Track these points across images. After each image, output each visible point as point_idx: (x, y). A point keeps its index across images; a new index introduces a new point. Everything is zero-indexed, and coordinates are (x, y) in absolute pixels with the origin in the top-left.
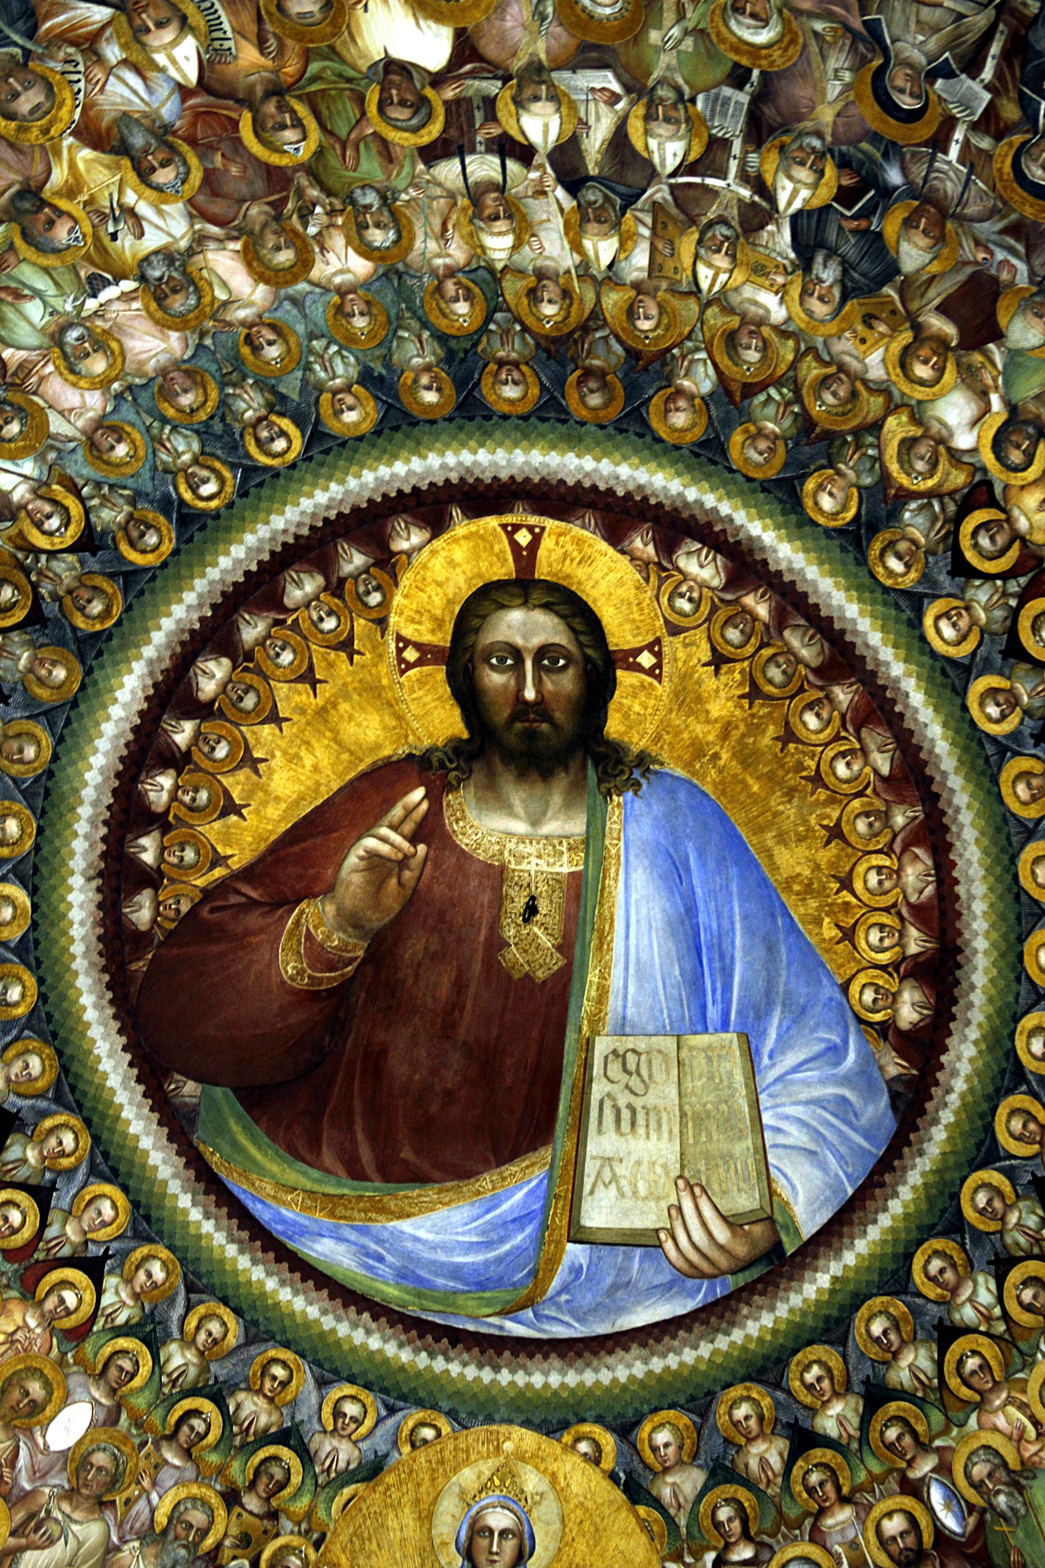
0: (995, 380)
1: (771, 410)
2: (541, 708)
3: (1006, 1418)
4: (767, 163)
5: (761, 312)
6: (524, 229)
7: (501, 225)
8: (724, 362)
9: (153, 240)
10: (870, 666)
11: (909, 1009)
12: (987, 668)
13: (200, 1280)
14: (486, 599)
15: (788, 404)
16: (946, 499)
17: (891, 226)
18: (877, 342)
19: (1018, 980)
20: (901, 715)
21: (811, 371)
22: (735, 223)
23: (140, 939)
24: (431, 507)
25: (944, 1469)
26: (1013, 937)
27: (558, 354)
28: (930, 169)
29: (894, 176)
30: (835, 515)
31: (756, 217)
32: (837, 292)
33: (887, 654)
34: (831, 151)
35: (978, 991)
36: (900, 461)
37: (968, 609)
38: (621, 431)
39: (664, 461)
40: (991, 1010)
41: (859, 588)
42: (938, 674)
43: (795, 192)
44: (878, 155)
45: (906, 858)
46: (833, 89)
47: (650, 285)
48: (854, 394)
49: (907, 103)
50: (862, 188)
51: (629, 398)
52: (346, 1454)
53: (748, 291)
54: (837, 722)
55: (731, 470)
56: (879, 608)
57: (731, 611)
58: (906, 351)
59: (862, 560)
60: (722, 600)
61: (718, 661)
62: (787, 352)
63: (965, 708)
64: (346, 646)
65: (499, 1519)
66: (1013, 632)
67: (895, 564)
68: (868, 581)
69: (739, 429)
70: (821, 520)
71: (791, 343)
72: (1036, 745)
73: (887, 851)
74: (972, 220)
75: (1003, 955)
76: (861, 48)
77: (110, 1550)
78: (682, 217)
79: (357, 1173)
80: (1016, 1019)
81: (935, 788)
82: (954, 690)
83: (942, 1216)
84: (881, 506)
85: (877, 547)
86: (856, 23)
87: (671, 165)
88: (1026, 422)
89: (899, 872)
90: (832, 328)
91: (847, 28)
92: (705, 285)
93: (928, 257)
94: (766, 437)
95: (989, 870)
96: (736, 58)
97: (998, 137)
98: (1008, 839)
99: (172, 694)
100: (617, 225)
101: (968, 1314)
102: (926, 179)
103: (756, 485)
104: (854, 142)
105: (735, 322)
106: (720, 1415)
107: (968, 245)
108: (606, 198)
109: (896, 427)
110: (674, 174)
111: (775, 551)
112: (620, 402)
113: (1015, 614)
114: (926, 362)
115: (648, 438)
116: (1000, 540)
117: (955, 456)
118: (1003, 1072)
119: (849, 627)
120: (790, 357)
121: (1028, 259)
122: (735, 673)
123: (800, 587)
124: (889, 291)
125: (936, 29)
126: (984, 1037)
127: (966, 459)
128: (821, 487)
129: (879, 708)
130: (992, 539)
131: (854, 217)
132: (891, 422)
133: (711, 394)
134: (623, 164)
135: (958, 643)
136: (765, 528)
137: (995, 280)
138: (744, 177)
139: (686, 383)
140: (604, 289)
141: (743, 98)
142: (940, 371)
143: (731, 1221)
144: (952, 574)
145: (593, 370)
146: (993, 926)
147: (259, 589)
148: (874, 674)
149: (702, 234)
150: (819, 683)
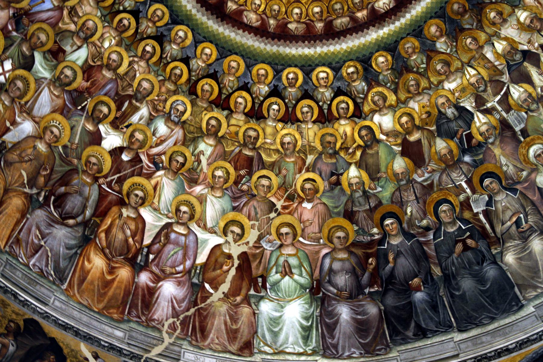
0: (390, 142)
1: (419, 61)
4: (493, 120)
5: (450, 80)
6: (522, 27)
7: (528, 21)
8: (442, 57)
10: (324, 41)
12: (305, 82)
15: (418, 68)
16: (362, 100)
17: (453, 145)
18: (421, 111)
19: (204, 37)
20: (304, 42)
21: (424, 83)
22: (482, 94)
26: (219, 43)
28: (463, 173)
29: (467, 159)
30: (376, 59)
31: (480, 102)
32: (443, 110)
33: (325, 49)
34: (486, 143)
35: (206, 20)
36: (381, 93)
37: (326, 86)
38: (441, 8)
39: (423, 15)
40: (199, 22)
41: (350, 53)
42: (311, 63)
43: (480, 121)
44: (476, 158)
45: (259, 17)
46: (503, 160)
47: (480, 51)
48: (409, 92)
49: (487, 182)
50: (469, 145)
51: (450, 18)
53: (459, 81)
54: (312, 18)
55: (408, 34)
56: (340, 56)
57: (365, 4)
58: (412, 118)
59: (358, 60)
60: (370, 3)
63: (296, 66)
66: (311, 98)
67: (351, 70)
68: (351, 57)
69: (419, 46)
70: (377, 54)
71: (436, 83)
72: (274, 85)
73: (264, 12)
74: (441, 175)
75: (214, 35)
76: (510, 181)
78: (494, 79)
80: (193, 30)
81: (276, 40)
82: (303, 66)
84: (371, 77)
85: (359, 67)
86: (518, 187)
87: (512, 90)
88: (372, 143)
89: (256, 12)
90: (433, 100)
91: (519, 183)
92: (469, 69)
93: (438, 150)
94: (412, 53)
95: (243, 45)
96: (531, 137)
97: (461, 203)
98: (249, 58)
100: (504, 57)
102: (461, 168)
103: (399, 40)
104: (484, 153)
105: (452, 69)
107: (435, 167)
108: (515, 60)
109: (392, 98)
110: (508, 87)
111: (376, 32)
112: (450, 14)
113: (317, 102)
114: (406, 122)
115: (433, 15)
116: (341, 111)
117: (373, 112)
118: (178, 16)
119: (340, 42)
120: (432, 79)
121: (420, 183)
123: (360, 33)
124: (434, 128)
125: (503, 212)
126: (191, 15)
127: (371, 115)
128: (387, 60)
129: (309, 36)
130: (343, 108)
131: (462, 134)
132: (394, 98)
133: (435, 45)
134: (522, 75)
135: (317, 76)
136: (384, 33)
137: (420, 167)
138: (494, 109)
139: (443, 40)
140: (487, 37)
141: (517, 129)
142: (401, 125)
144: (339, 88)
146: (225, 37)
148: (321, 41)
149: (485, 81)
150: (327, 20)
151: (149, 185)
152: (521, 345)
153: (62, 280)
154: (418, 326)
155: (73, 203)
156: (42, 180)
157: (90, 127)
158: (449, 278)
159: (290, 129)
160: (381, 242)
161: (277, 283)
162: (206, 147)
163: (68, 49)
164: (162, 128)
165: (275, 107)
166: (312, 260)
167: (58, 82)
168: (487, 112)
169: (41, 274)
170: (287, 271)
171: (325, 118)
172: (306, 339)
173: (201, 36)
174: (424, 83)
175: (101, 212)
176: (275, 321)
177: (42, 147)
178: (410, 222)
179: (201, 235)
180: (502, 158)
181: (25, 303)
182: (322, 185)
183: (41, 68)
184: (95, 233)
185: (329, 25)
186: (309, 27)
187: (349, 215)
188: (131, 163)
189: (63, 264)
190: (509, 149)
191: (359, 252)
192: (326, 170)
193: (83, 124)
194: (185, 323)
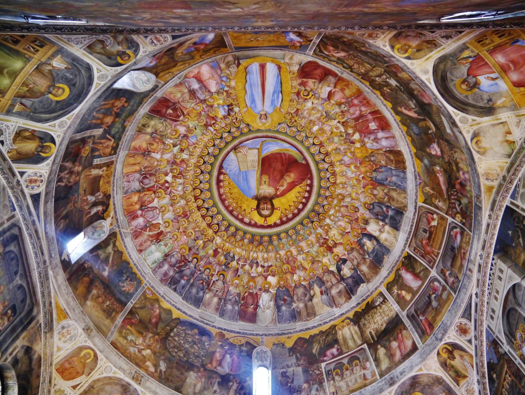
2: (264, 203)
3: (206, 139)
4: (237, 266)
6: (263, 257)
9: (302, 256)
11: (222, 177)
13: (302, 142)
14: (270, 216)
17: (224, 261)
21: (234, 243)
23: (309, 179)
24: (276, 225)
25: (212, 133)
27: (260, 243)
29: (223, 267)
31: (239, 260)
43: (234, 263)
50: (227, 265)
52: (283, 125)
61: (245, 210)
62: (237, 245)
64: (285, 209)
65: (264, 120)
77: (309, 116)
79: (284, 154)
83: (216, 157)
99: (305, 205)
101: (212, 148)
106: (239, 133)
109: (225, 238)
122: (243, 209)
129: (227, 208)
143: (240, 152)
145: (257, 241)
147: (295, 216)
151: (164, 195)
152: (190, 316)
153: (125, 194)
154: (176, 288)
155: (146, 181)
156: (147, 169)
157: (168, 171)
158: (192, 285)
159: (201, 219)
160: (189, 262)
161: (160, 245)
162: (183, 202)
163: (185, 152)
164: (180, 188)
165: (204, 212)
166: (173, 249)
167: (175, 156)
168: (238, 263)
169: (123, 188)
170: (166, 245)
171: (209, 225)
172: (153, 263)
173: (209, 182)
174: (234, 243)
175: (149, 189)
176: (152, 252)
177: (156, 163)
178: (198, 266)
179: (160, 218)
180: (229, 275)
181: (113, 190)
182: (193, 237)
183: (176, 150)
184: (143, 192)
185: (233, 210)
186: (229, 206)
187: (190, 249)
188: (166, 187)
189: (129, 191)
190: (233, 275)
191: (183, 259)
192: (197, 235)
193: (168, 169)
194: (135, 231)
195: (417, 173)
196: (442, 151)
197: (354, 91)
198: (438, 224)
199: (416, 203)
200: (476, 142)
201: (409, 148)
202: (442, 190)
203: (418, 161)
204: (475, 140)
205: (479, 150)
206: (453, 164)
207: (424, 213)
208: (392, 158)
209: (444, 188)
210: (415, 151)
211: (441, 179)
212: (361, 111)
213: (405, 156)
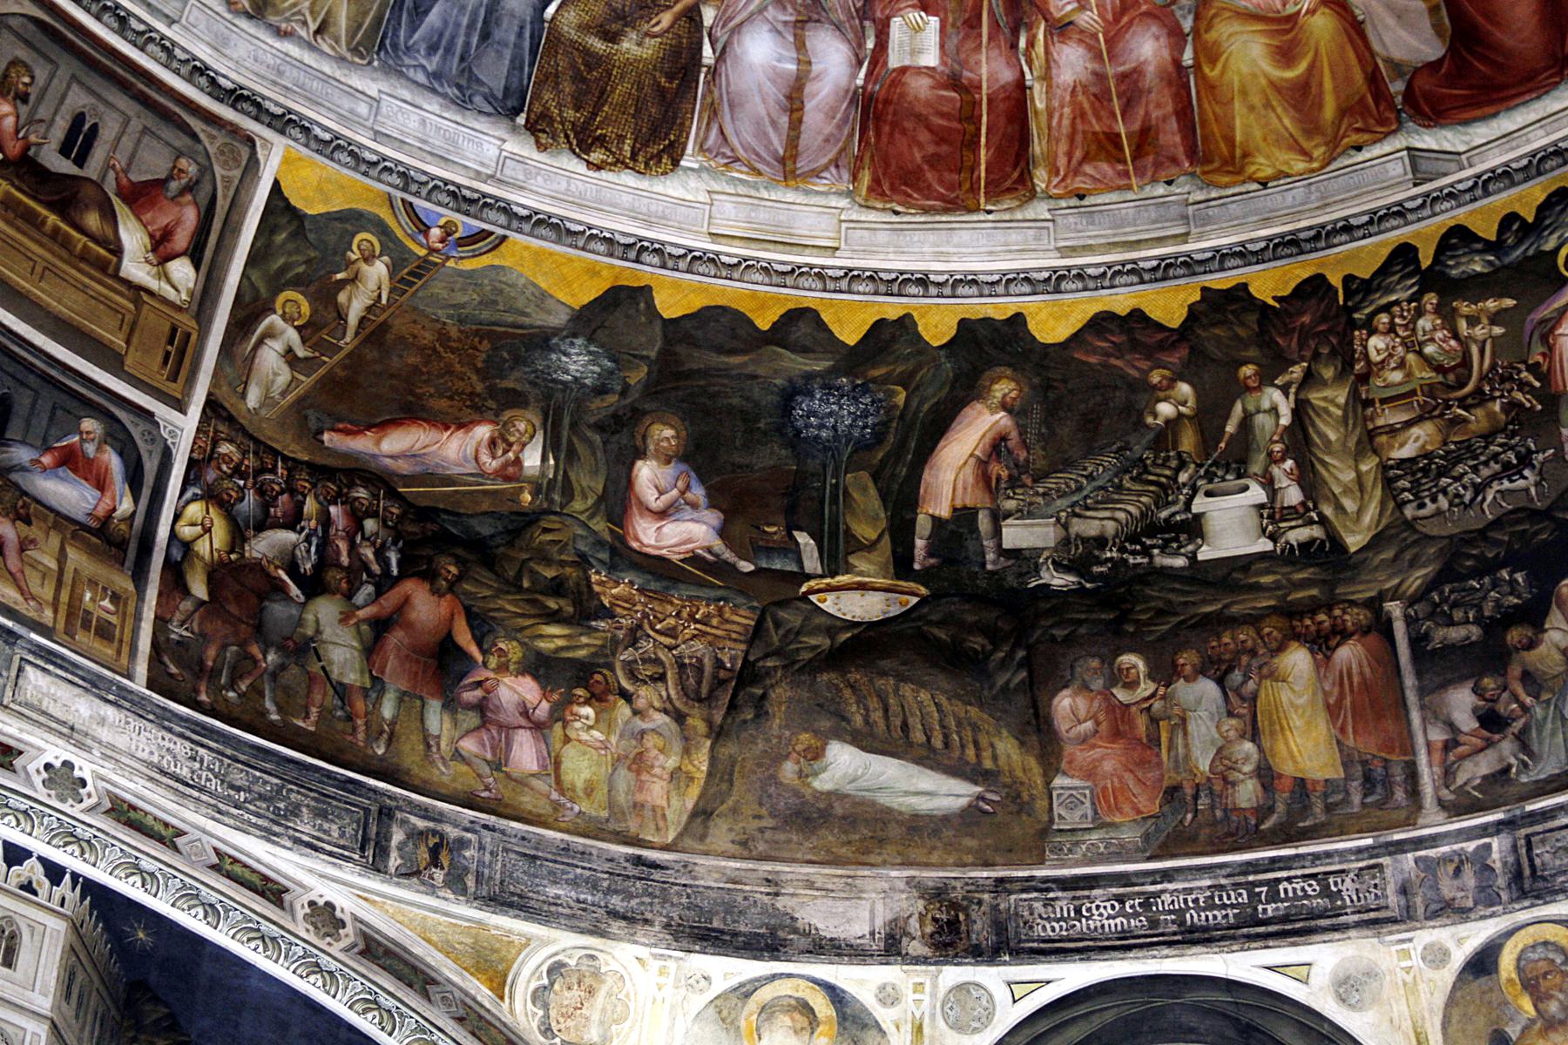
195: (493, 223)
196: (659, 570)
197: (1244, 124)
198: (136, 290)
199: (284, 122)
200: (805, 1008)
201: (695, 259)
202: (383, 426)
203: (588, 293)
204: (822, 1006)
205: (753, 1003)
206: (585, 646)
207: (206, 170)
208: (629, 46)
209: (396, 446)
210: (670, 305)
211: (459, 449)
212: (1062, 29)
213: (628, 178)
